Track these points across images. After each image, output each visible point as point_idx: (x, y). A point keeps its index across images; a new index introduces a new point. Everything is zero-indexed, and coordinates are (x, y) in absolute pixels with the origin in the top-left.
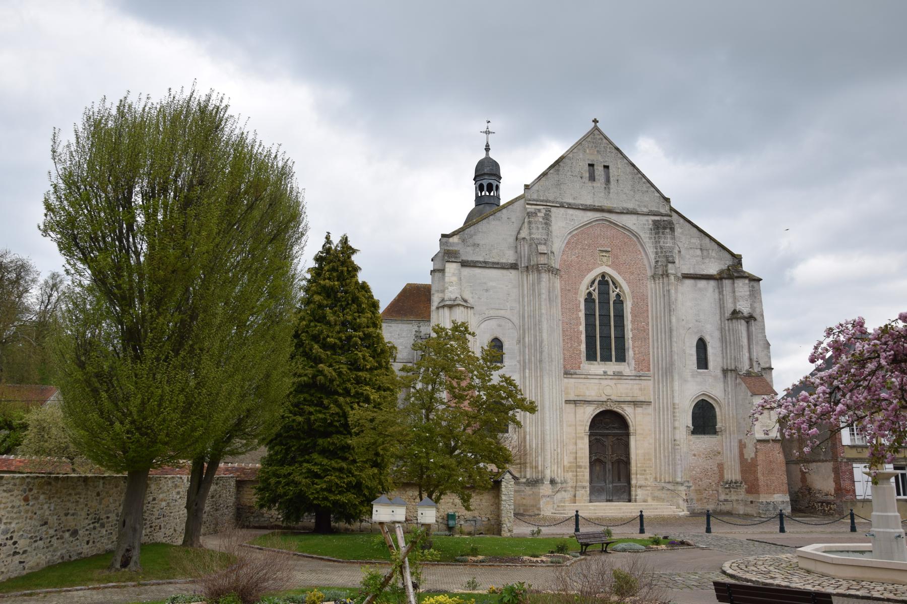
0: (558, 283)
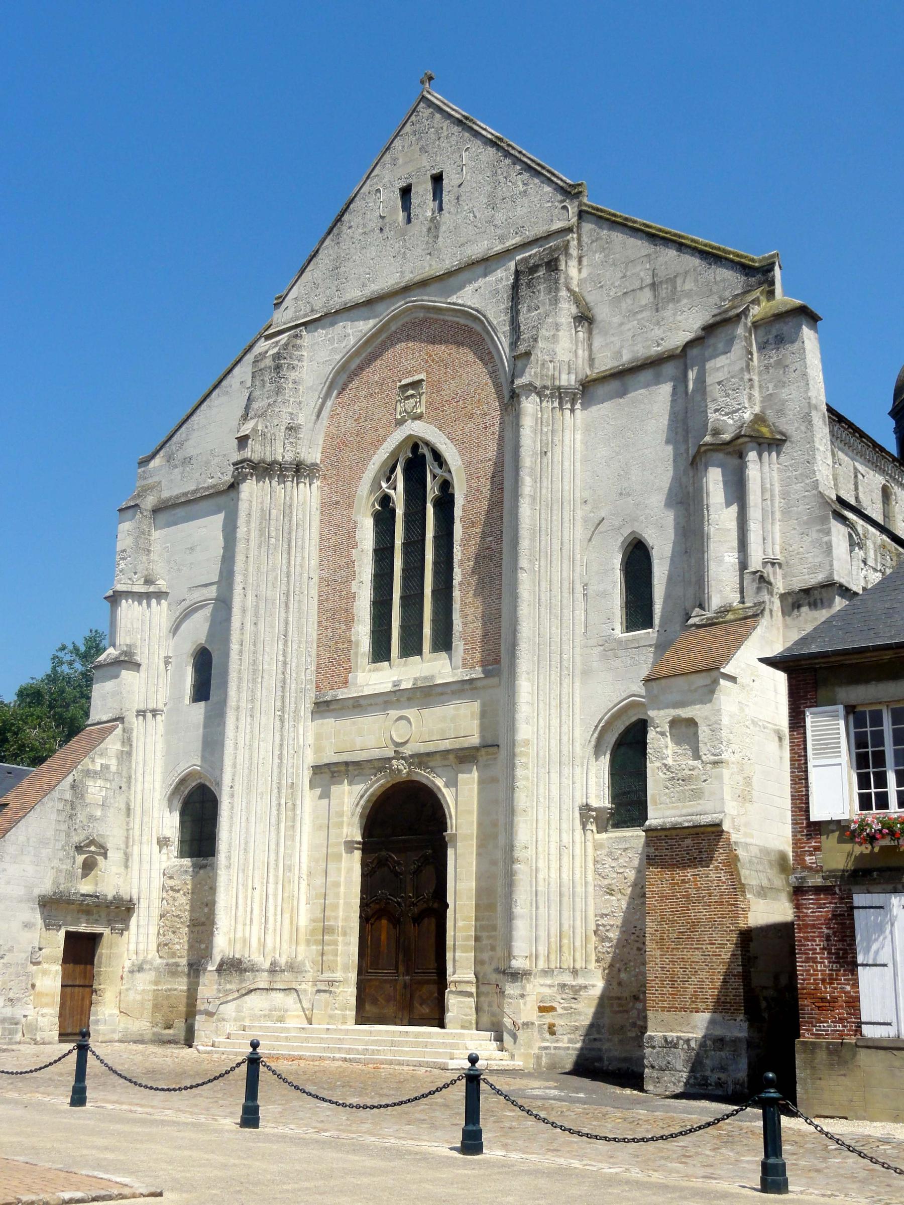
0: (308, 496)
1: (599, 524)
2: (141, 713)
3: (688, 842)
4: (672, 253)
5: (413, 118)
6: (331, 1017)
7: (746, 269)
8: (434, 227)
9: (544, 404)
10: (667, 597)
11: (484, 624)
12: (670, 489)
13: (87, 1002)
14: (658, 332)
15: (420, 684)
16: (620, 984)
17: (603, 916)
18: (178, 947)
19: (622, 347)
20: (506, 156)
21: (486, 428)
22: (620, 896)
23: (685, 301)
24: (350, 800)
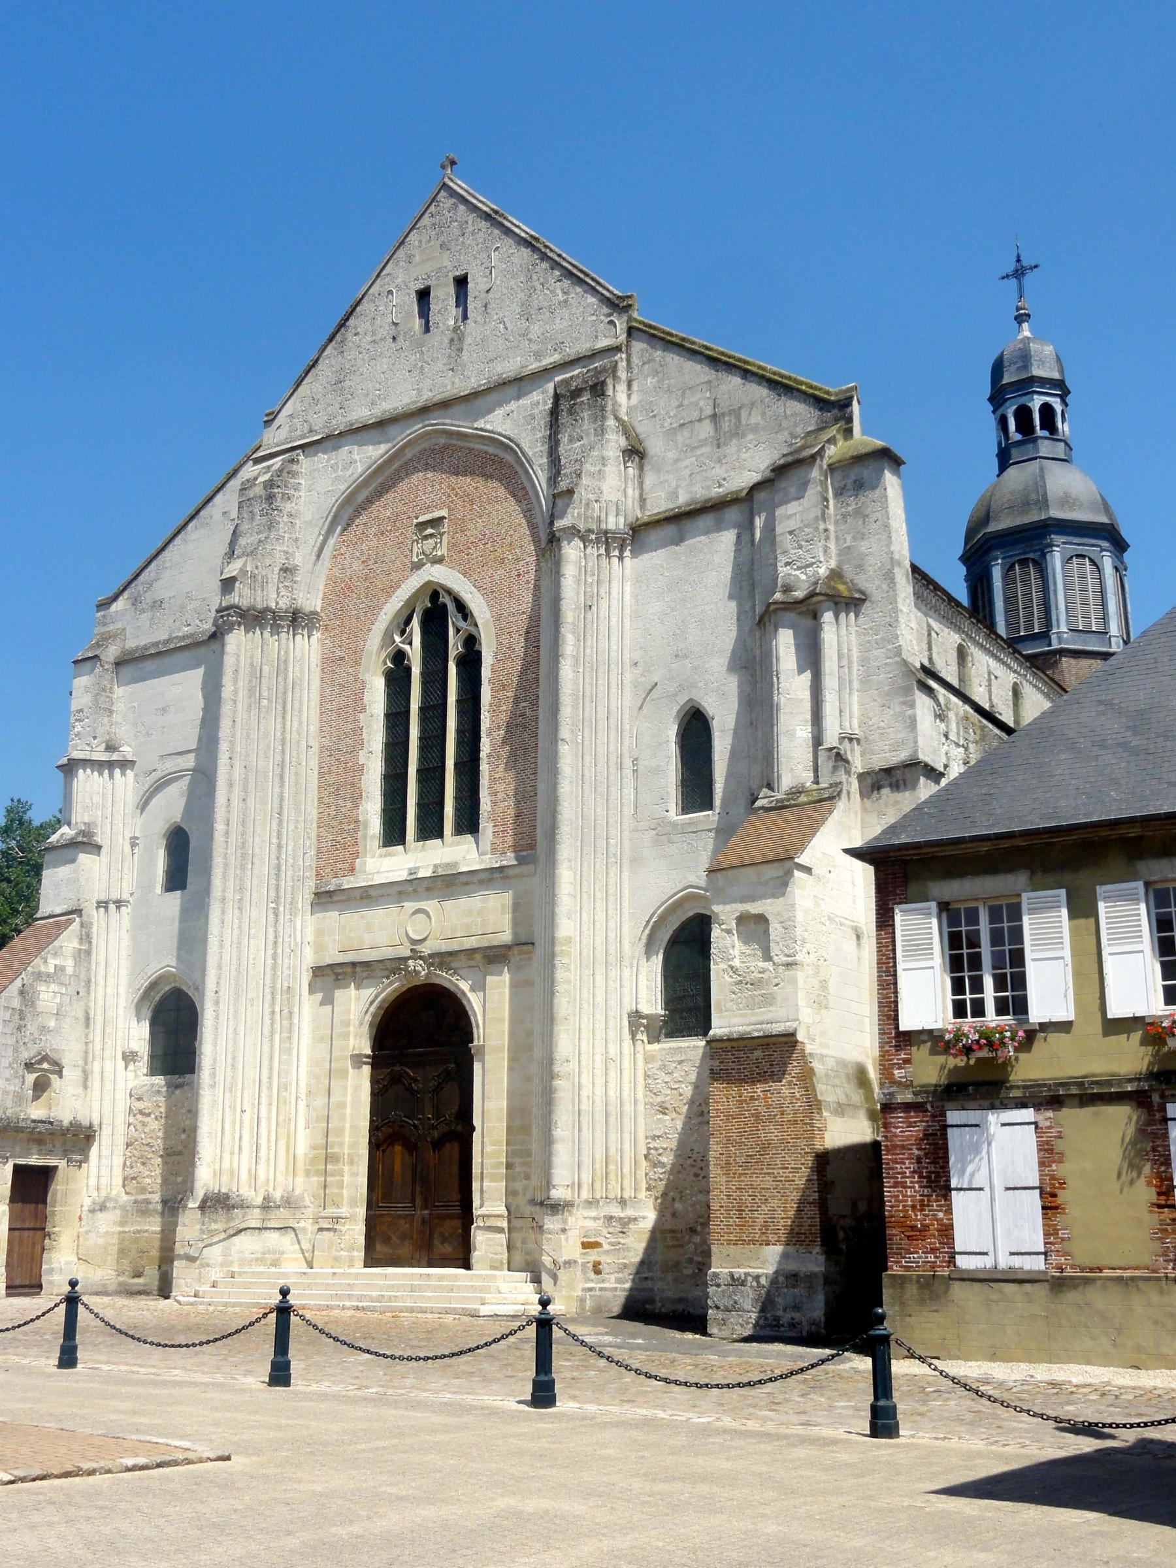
0: (307, 649)
1: (651, 690)
2: (103, 904)
3: (758, 1053)
4: (736, 380)
5: (432, 208)
6: (336, 1259)
7: (820, 403)
8: (457, 339)
9: (589, 550)
10: (730, 776)
11: (517, 803)
12: (733, 651)
13: (39, 1248)
14: (719, 471)
15: (441, 872)
16: (674, 1215)
17: (655, 1138)
18: (148, 1181)
19: (677, 487)
20: (542, 260)
21: (519, 576)
22: (674, 1115)
23: (750, 437)
24: (358, 1006)
